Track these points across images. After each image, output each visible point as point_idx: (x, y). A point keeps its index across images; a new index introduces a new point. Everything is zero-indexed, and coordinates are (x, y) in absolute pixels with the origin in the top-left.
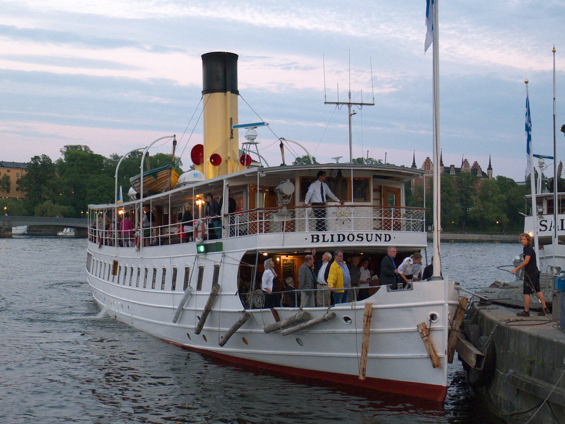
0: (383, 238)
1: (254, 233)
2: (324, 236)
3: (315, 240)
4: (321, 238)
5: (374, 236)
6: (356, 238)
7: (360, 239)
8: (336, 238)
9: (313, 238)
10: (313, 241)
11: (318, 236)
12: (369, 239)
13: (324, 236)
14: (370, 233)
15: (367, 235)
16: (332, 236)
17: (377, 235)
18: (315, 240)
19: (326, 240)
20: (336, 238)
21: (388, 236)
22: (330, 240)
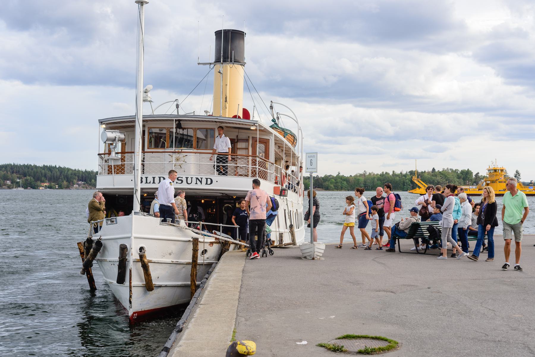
0: (204, 181)
2: (147, 178)
5: (194, 180)
7: (180, 182)
13: (147, 178)
15: (187, 178)
16: (154, 178)
17: (197, 178)
19: (148, 182)
22: (152, 182)
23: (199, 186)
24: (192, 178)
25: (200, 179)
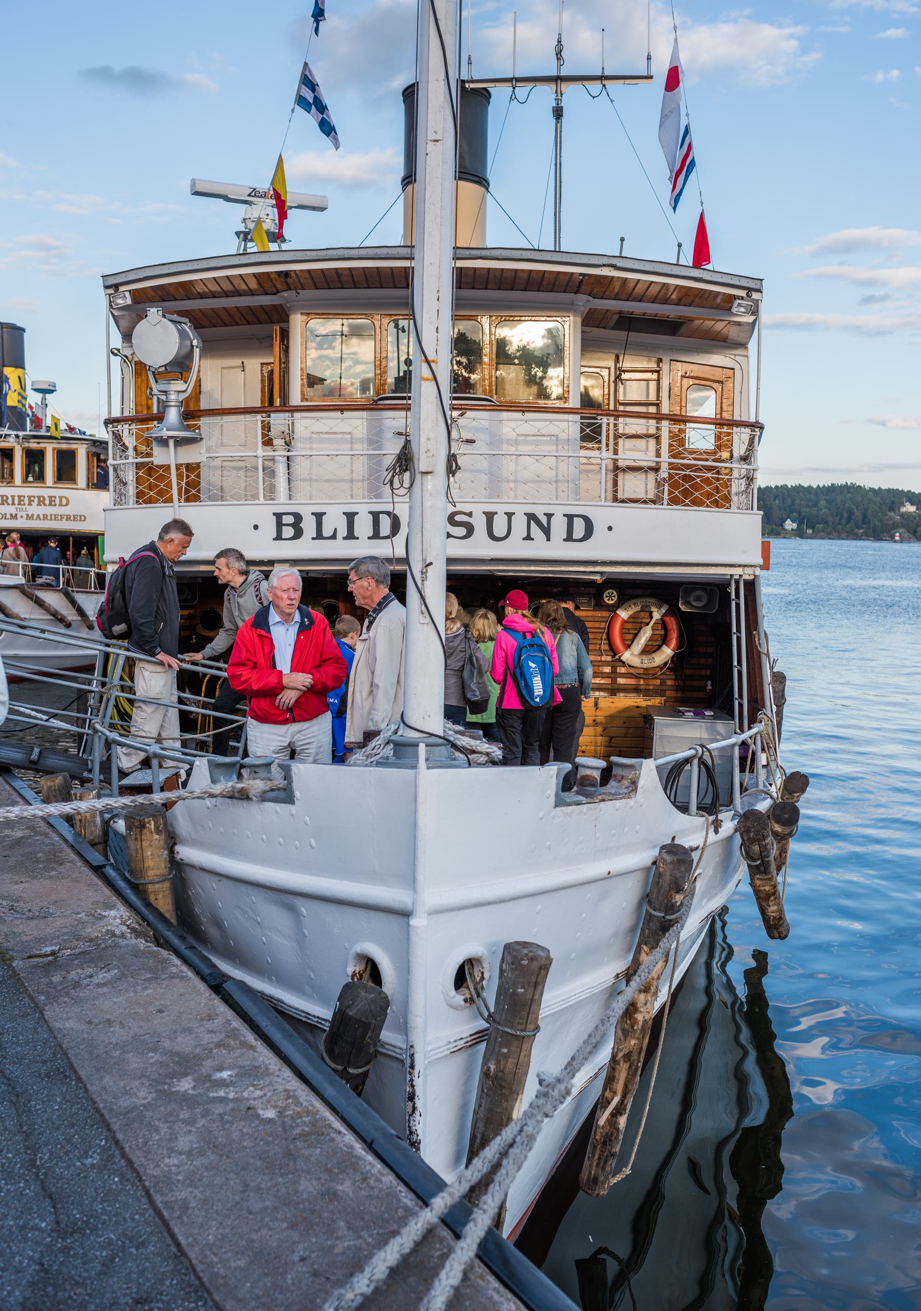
0: (559, 527)
1: (716, 504)
2: (319, 516)
3: (288, 532)
5: (519, 523)
7: (462, 531)
8: (364, 526)
9: (280, 525)
10: (279, 537)
11: (298, 517)
13: (319, 516)
14: (501, 509)
15: (490, 516)
16: (350, 517)
17: (531, 517)
19: (327, 532)
20: (364, 526)
22: (343, 532)
23: (540, 548)
24: (510, 515)
25: (544, 520)
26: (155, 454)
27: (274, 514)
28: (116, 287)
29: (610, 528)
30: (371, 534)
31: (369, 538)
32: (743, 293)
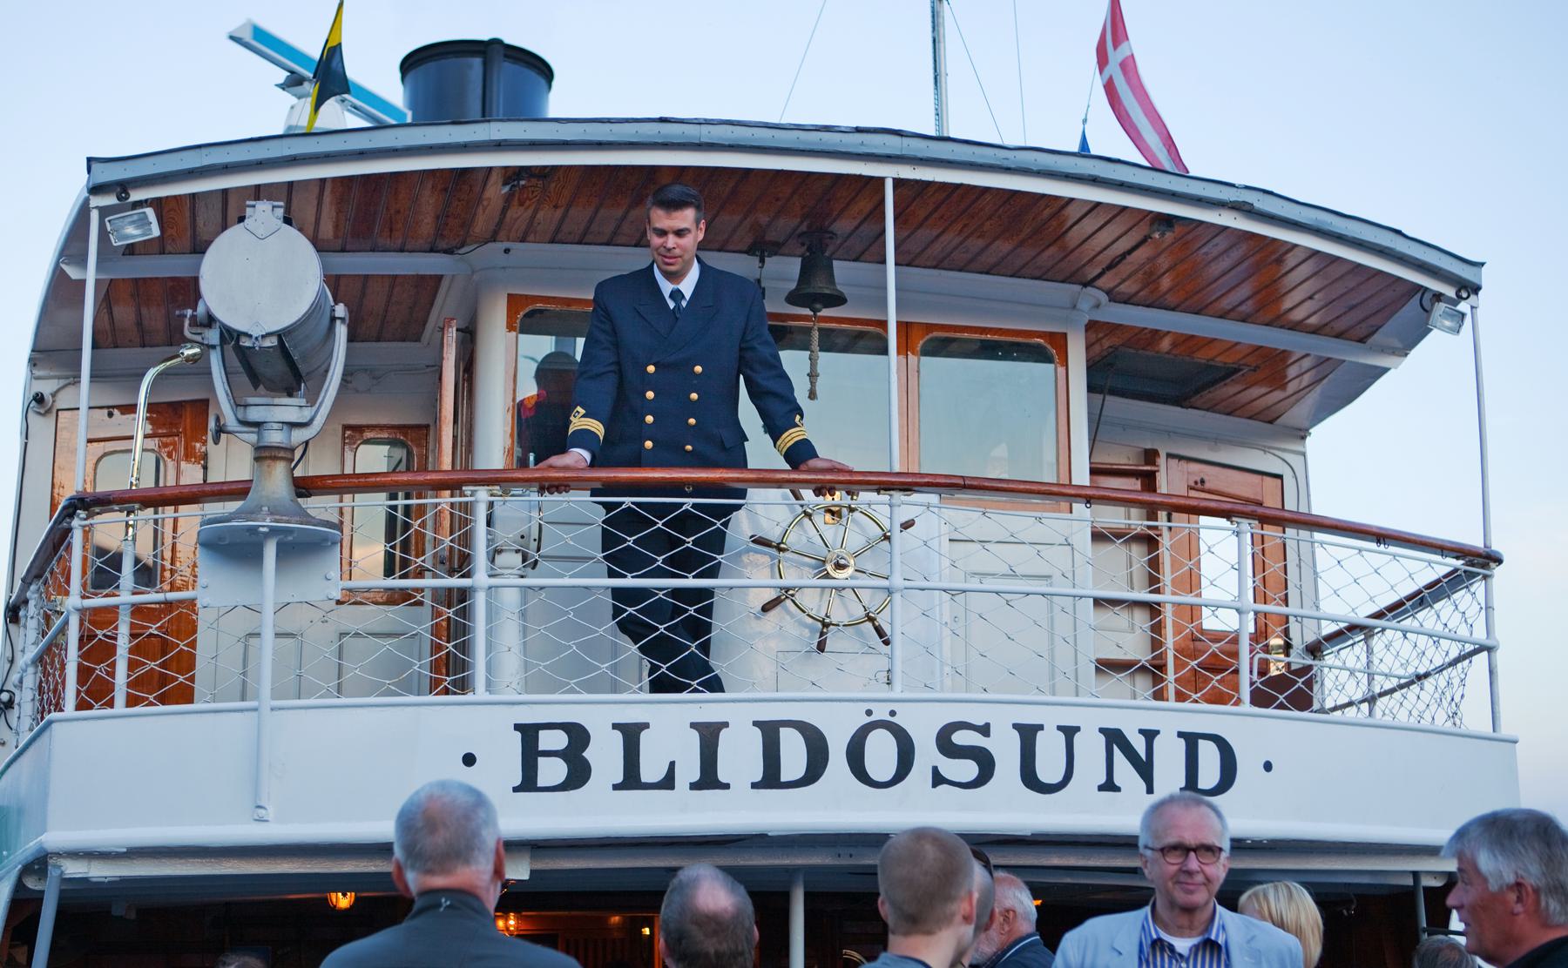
2: (631, 734)
3: (552, 771)
4: (605, 755)
5: (1090, 749)
6: (927, 755)
7: (967, 769)
8: (740, 757)
10: (528, 783)
11: (578, 736)
12: (1049, 771)
13: (631, 734)
14: (1050, 719)
15: (1028, 733)
16: (709, 735)
17: (1114, 738)
18: (552, 771)
19: (651, 770)
20: (740, 757)
21: (1209, 756)
22: (689, 770)
24: (1069, 732)
25: (1139, 744)
26: (201, 581)
27: (517, 727)
28: (122, 188)
29: (1268, 766)
30: (758, 777)
31: (754, 786)
32: (1450, 292)
